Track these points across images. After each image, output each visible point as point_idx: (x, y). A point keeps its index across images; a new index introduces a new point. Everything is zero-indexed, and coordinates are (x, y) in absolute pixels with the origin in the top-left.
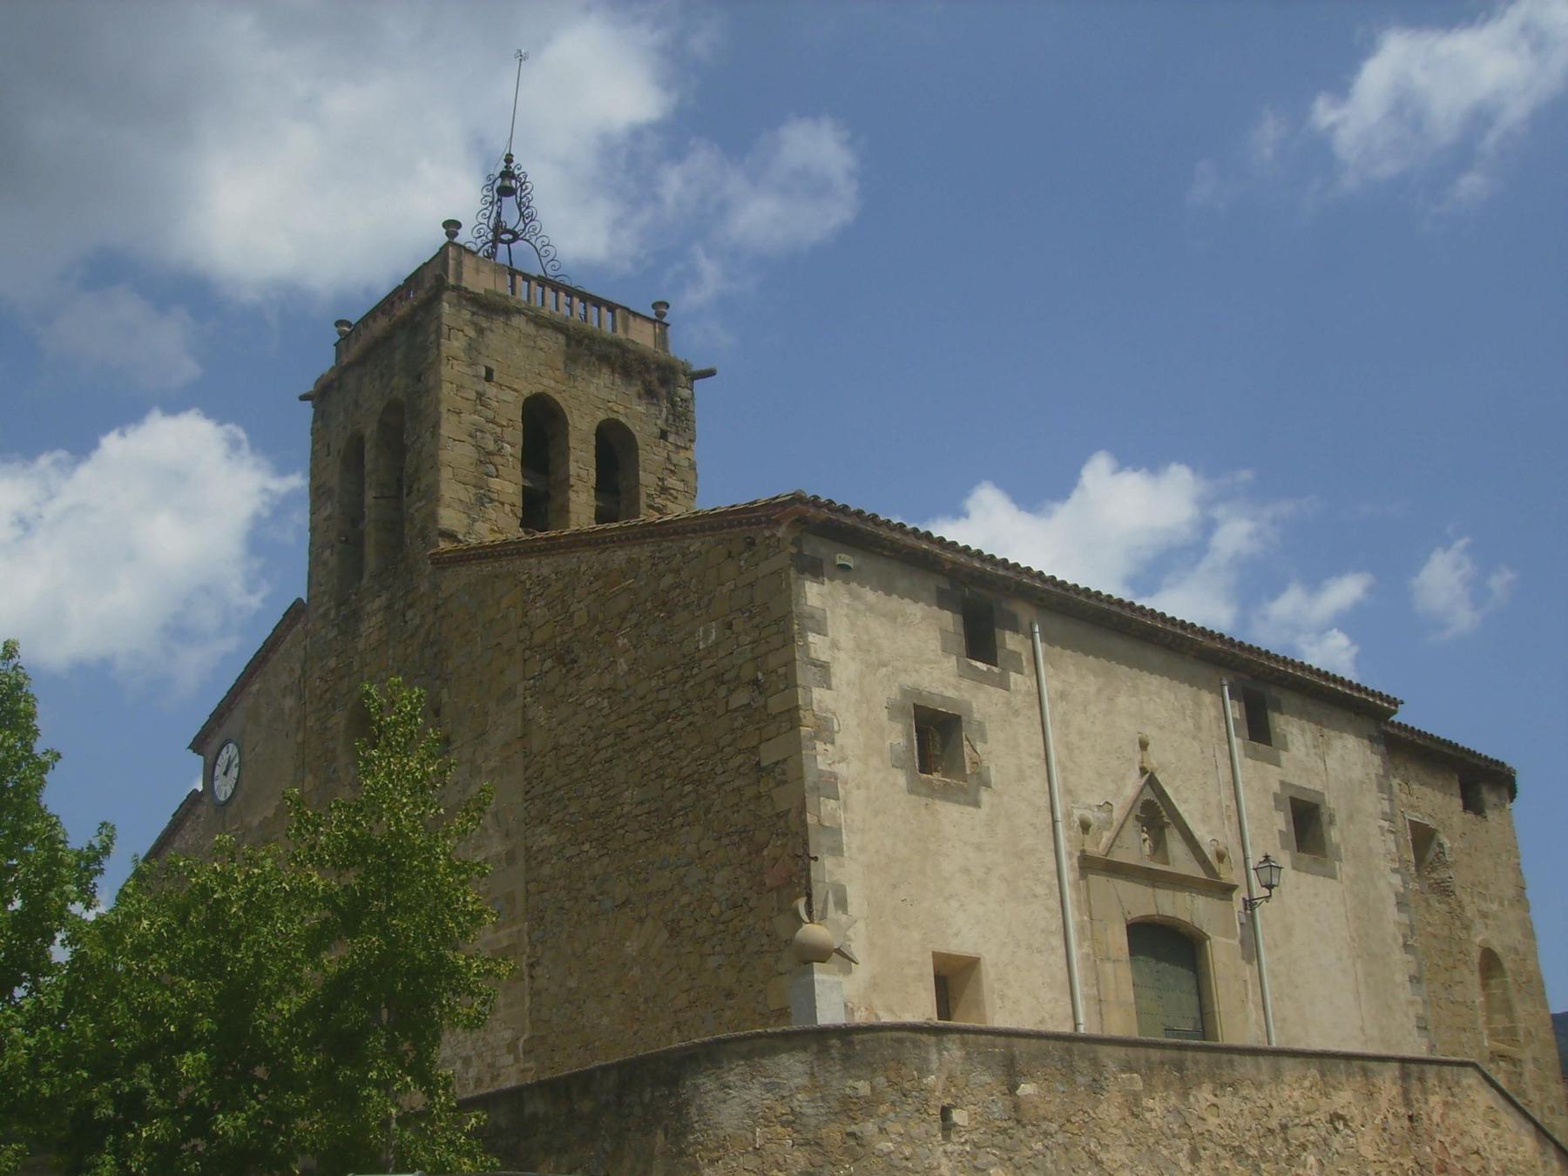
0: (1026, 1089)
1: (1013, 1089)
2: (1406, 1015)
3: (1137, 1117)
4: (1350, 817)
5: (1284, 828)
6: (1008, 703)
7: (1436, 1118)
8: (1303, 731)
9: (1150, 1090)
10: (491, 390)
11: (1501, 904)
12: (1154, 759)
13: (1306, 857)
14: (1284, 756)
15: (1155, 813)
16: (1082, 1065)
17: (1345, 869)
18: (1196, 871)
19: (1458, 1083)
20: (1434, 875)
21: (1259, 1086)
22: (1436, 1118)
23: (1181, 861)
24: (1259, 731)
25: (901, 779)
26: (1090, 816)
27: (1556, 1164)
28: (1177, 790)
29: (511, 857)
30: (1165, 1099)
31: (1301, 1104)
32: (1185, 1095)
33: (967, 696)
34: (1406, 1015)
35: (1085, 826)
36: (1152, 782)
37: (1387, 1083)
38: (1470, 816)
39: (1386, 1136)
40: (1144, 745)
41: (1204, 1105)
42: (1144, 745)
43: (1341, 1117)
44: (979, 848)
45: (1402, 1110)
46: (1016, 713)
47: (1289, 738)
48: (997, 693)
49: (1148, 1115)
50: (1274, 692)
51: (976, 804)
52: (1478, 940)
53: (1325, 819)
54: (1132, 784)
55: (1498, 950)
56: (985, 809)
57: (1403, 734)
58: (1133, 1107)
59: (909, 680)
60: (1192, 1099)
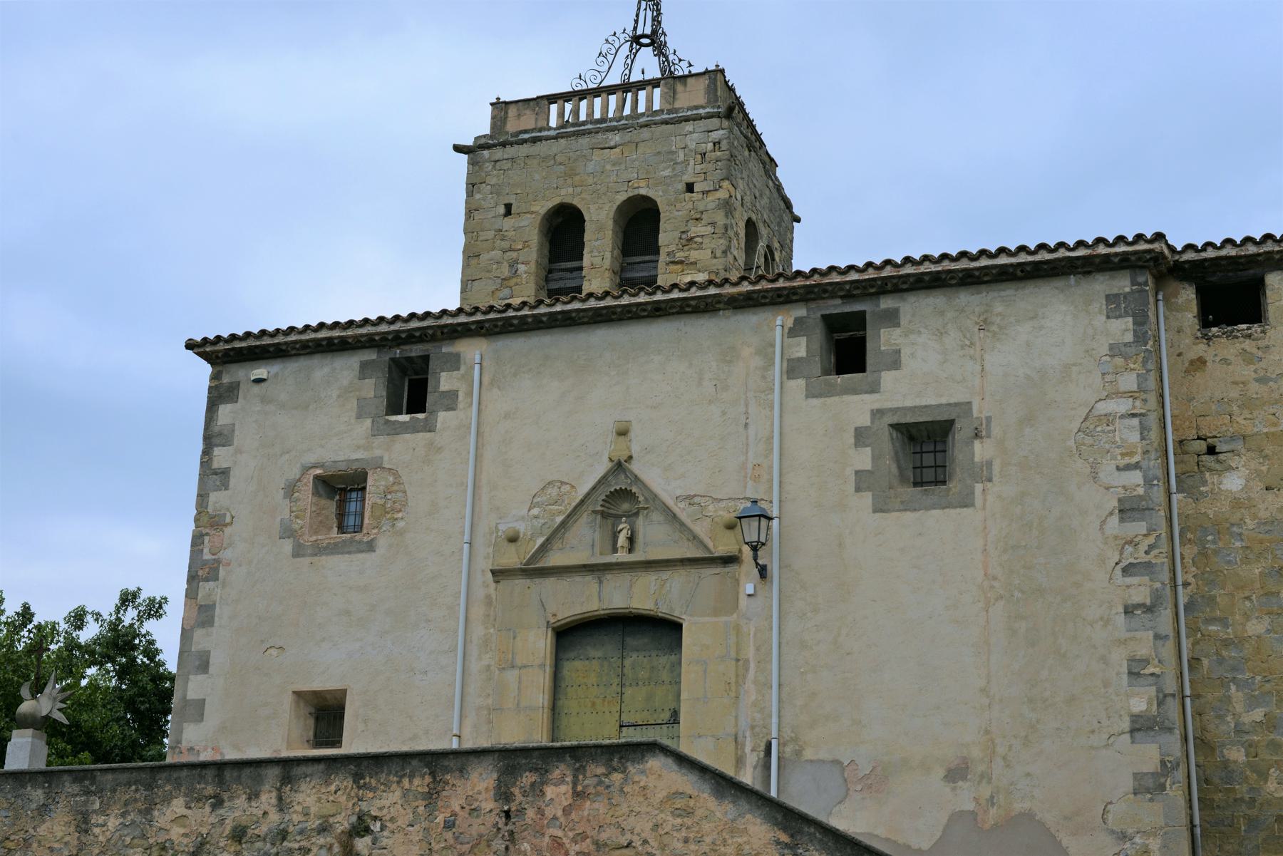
2: (1104, 660)
3: (86, 831)
5: (867, 465)
6: (431, 444)
7: (555, 810)
8: (941, 334)
10: (509, 223)
22: (555, 810)
26: (522, 527)
30: (123, 815)
31: (313, 810)
32: (147, 812)
33: (377, 453)
34: (1104, 660)
37: (480, 782)
39: (449, 835)
42: (623, 433)
46: (440, 450)
47: (905, 353)
49: (97, 831)
58: (83, 824)
59: (311, 459)
60: (156, 813)
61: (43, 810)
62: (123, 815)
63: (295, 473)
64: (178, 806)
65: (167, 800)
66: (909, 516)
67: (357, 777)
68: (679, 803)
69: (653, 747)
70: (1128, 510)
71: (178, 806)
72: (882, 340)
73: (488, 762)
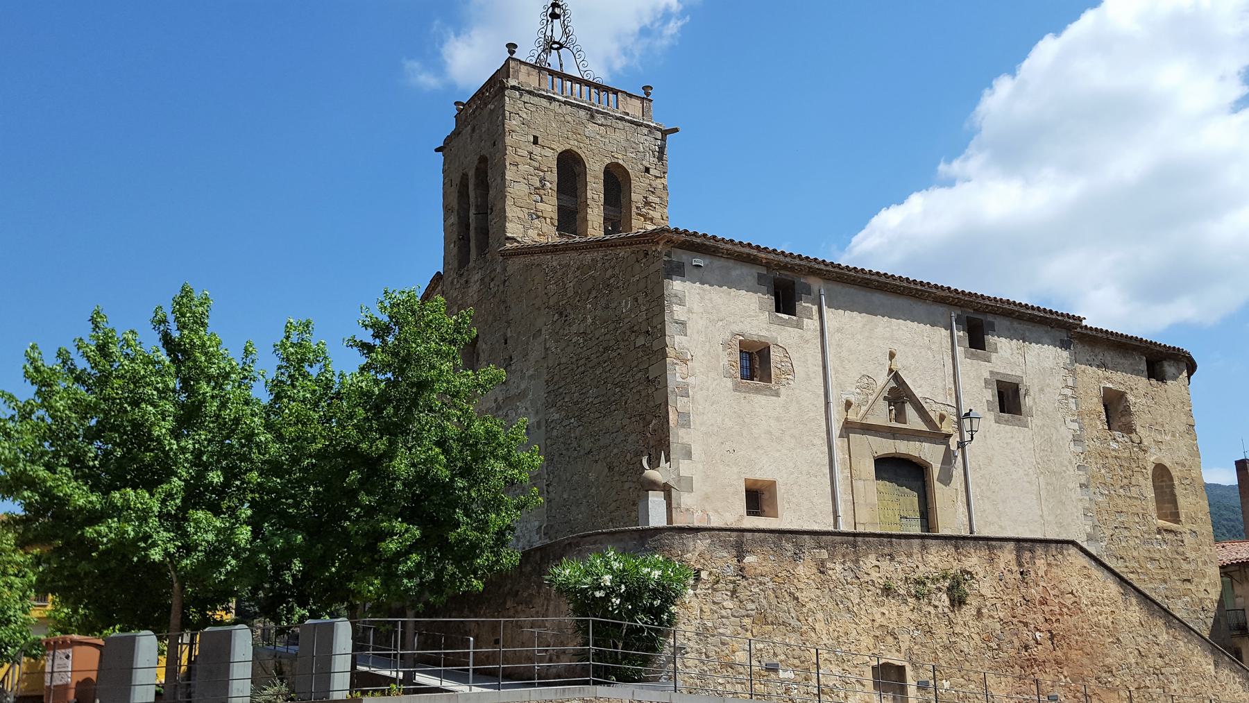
0: (749, 559)
1: (740, 557)
4: (1042, 390)
7: (1041, 573)
9: (832, 557)
11: (1173, 436)
12: (897, 365)
13: (1006, 415)
14: (994, 356)
15: (899, 395)
16: (789, 546)
17: (1035, 422)
18: (922, 426)
19: (1062, 553)
20: (1123, 419)
21: (910, 555)
22: (1041, 573)
23: (914, 421)
24: (977, 342)
25: (729, 383)
26: (852, 399)
27: (1134, 601)
28: (915, 380)
29: (539, 423)
30: (843, 563)
32: (857, 561)
35: (848, 405)
36: (896, 377)
37: (1007, 556)
38: (1153, 381)
40: (892, 356)
41: (870, 566)
42: (892, 356)
43: (968, 573)
44: (778, 419)
45: (1015, 568)
47: (999, 345)
48: (794, 332)
49: (830, 572)
50: (990, 318)
51: (777, 395)
52: (1152, 459)
53: (1022, 392)
54: (882, 380)
55: (1168, 464)
56: (783, 397)
57: (1100, 335)
61: (796, 557)
62: (843, 563)
63: (728, 336)
64: (872, 560)
65: (866, 555)
66: (1008, 427)
67: (957, 548)
68: (1085, 572)
69: (1073, 543)
70: (1077, 440)
71: (872, 560)
72: (991, 339)
73: (1011, 545)
